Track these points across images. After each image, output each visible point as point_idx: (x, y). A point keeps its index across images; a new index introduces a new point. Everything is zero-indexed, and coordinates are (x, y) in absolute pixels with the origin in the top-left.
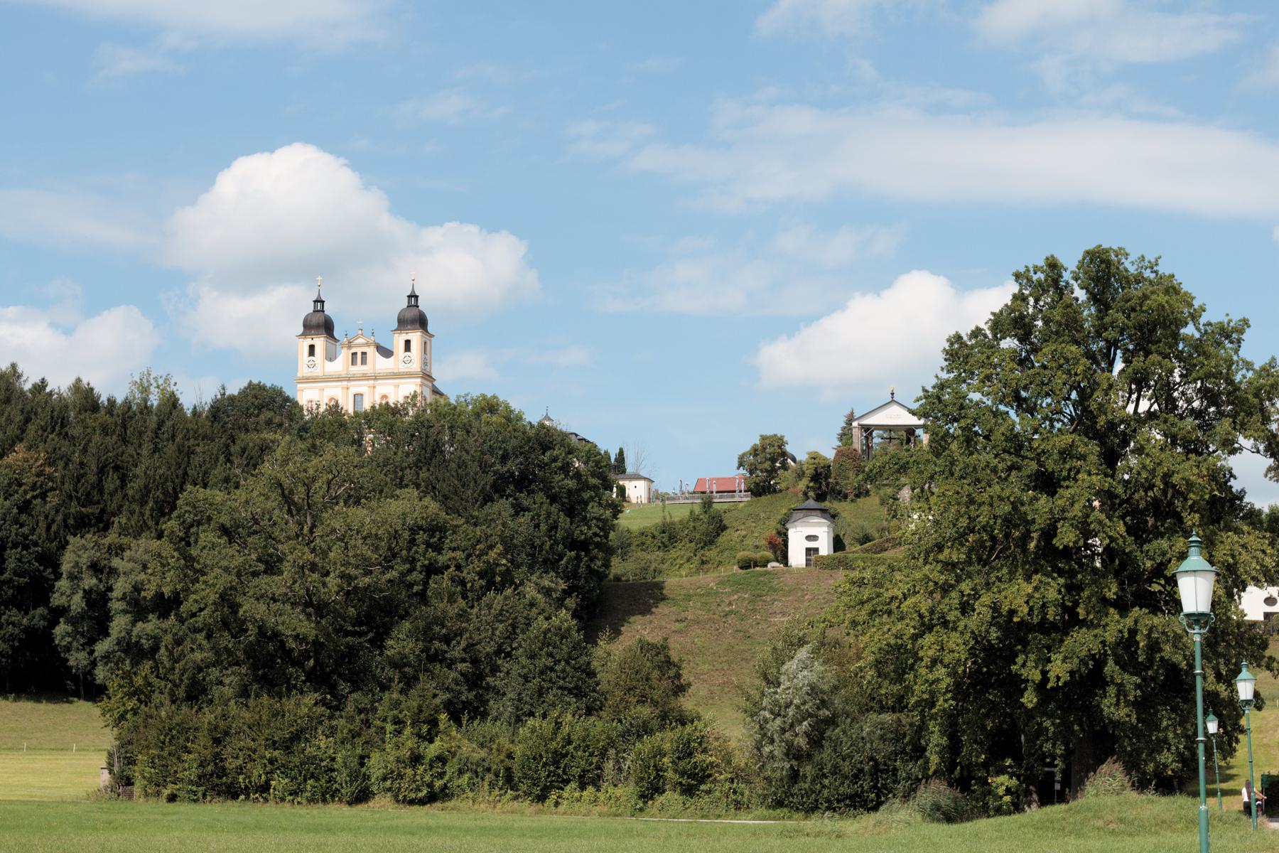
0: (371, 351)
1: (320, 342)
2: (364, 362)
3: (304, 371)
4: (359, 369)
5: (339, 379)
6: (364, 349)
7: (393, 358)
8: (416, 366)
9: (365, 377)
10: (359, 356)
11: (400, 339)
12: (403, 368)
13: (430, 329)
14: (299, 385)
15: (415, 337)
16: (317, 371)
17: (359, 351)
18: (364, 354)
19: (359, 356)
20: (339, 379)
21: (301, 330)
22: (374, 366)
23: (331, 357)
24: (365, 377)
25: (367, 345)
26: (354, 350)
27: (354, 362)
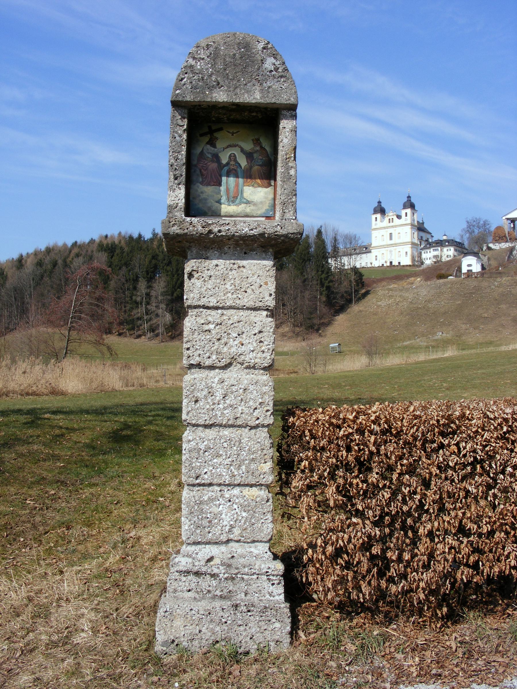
0: (395, 218)
1: (378, 216)
2: (393, 222)
4: (391, 224)
5: (384, 228)
8: (409, 221)
9: (393, 227)
10: (391, 220)
11: (403, 212)
12: (405, 223)
13: (416, 208)
15: (409, 211)
17: (391, 218)
19: (391, 220)
20: (384, 228)
24: (393, 227)
25: (393, 215)
26: (389, 218)
27: (389, 222)
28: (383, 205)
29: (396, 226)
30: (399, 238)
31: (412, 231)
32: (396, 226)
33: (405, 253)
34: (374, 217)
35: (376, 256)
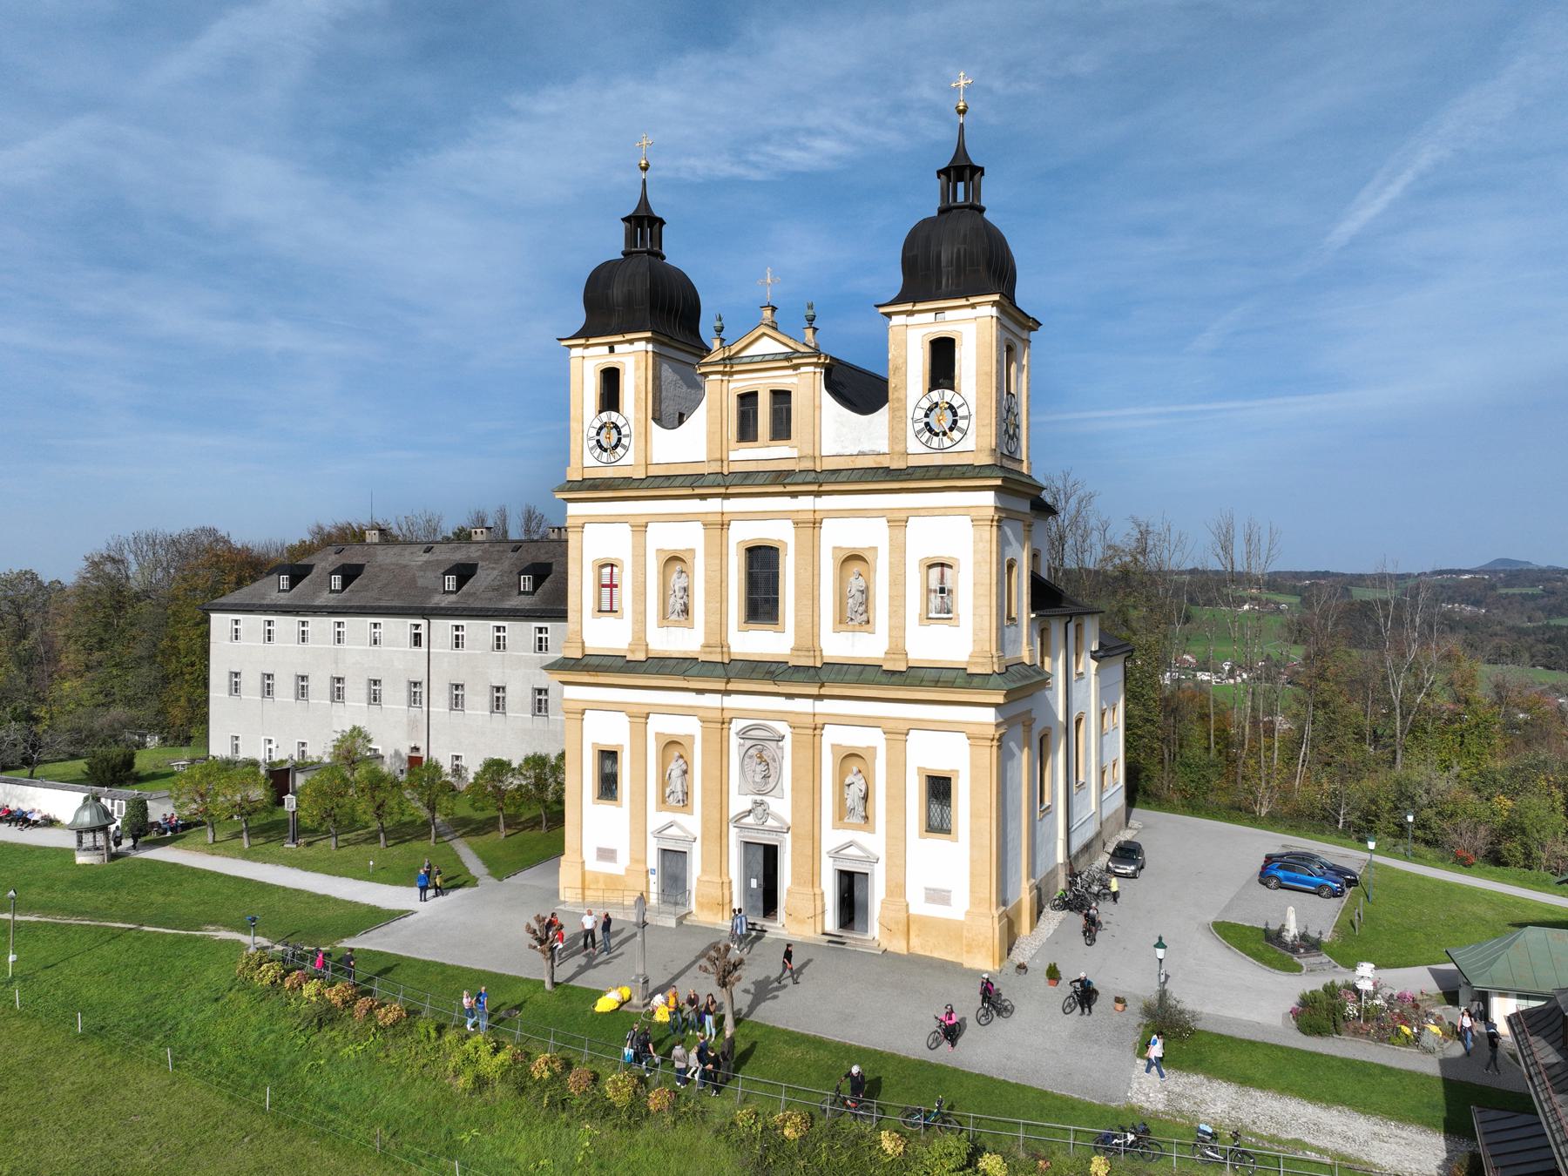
0: (806, 384)
2: (782, 429)
3: (587, 461)
4: (765, 453)
7: (883, 414)
9: (781, 481)
12: (918, 450)
14: (573, 509)
16: (628, 462)
17: (763, 383)
18: (781, 398)
21: (579, 318)
22: (816, 441)
23: (669, 414)
24: (781, 481)
26: (742, 384)
27: (747, 431)
28: (677, 252)
29: (823, 480)
30: (855, 612)
31: (1003, 543)
32: (823, 480)
33: (915, 792)
34: (588, 362)
35: (608, 756)
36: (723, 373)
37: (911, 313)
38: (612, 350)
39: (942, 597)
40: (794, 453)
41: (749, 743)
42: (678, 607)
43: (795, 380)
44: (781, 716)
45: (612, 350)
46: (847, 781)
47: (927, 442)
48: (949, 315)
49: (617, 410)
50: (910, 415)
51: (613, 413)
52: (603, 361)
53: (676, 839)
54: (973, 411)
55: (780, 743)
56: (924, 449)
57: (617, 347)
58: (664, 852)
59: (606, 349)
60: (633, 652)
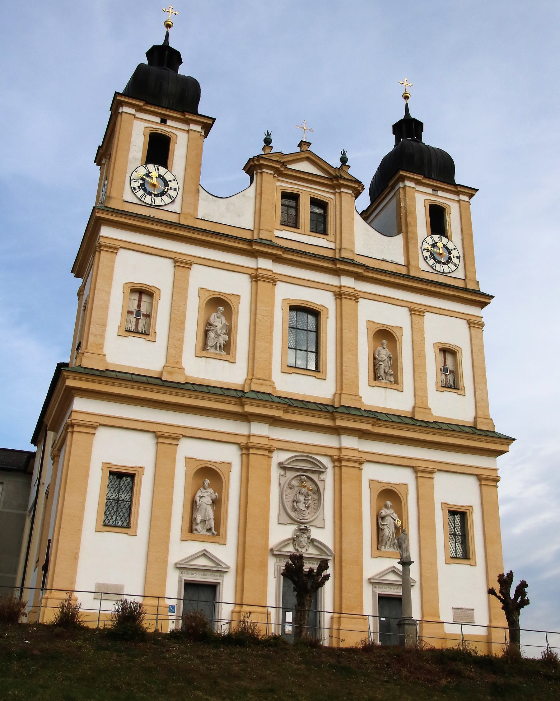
6: (324, 194)
36: (277, 171)
37: (418, 182)
38: (164, 121)
39: (446, 375)
40: (332, 246)
41: (291, 475)
42: (222, 340)
43: (332, 196)
44: (324, 451)
45: (164, 121)
46: (384, 512)
47: (433, 265)
48: (441, 193)
49: (165, 165)
50: (420, 246)
51: (161, 168)
52: (155, 126)
53: (204, 570)
54: (461, 256)
55: (322, 477)
56: (430, 270)
57: (169, 122)
58: (189, 586)
59: (158, 120)
60: (170, 373)
